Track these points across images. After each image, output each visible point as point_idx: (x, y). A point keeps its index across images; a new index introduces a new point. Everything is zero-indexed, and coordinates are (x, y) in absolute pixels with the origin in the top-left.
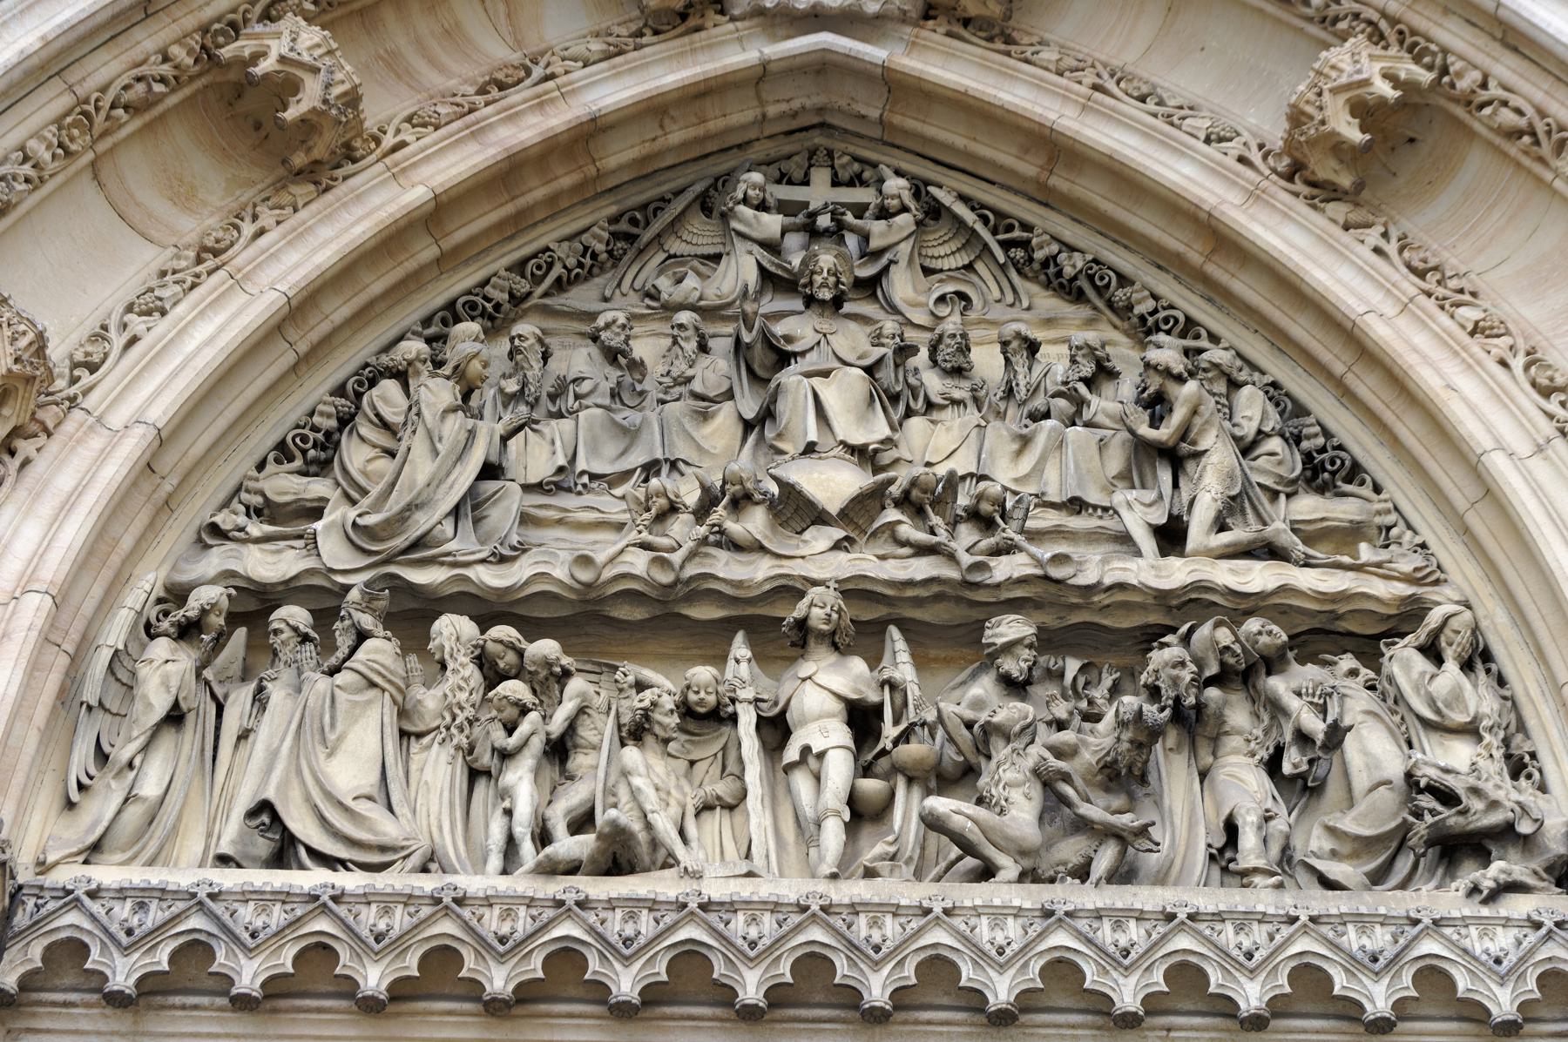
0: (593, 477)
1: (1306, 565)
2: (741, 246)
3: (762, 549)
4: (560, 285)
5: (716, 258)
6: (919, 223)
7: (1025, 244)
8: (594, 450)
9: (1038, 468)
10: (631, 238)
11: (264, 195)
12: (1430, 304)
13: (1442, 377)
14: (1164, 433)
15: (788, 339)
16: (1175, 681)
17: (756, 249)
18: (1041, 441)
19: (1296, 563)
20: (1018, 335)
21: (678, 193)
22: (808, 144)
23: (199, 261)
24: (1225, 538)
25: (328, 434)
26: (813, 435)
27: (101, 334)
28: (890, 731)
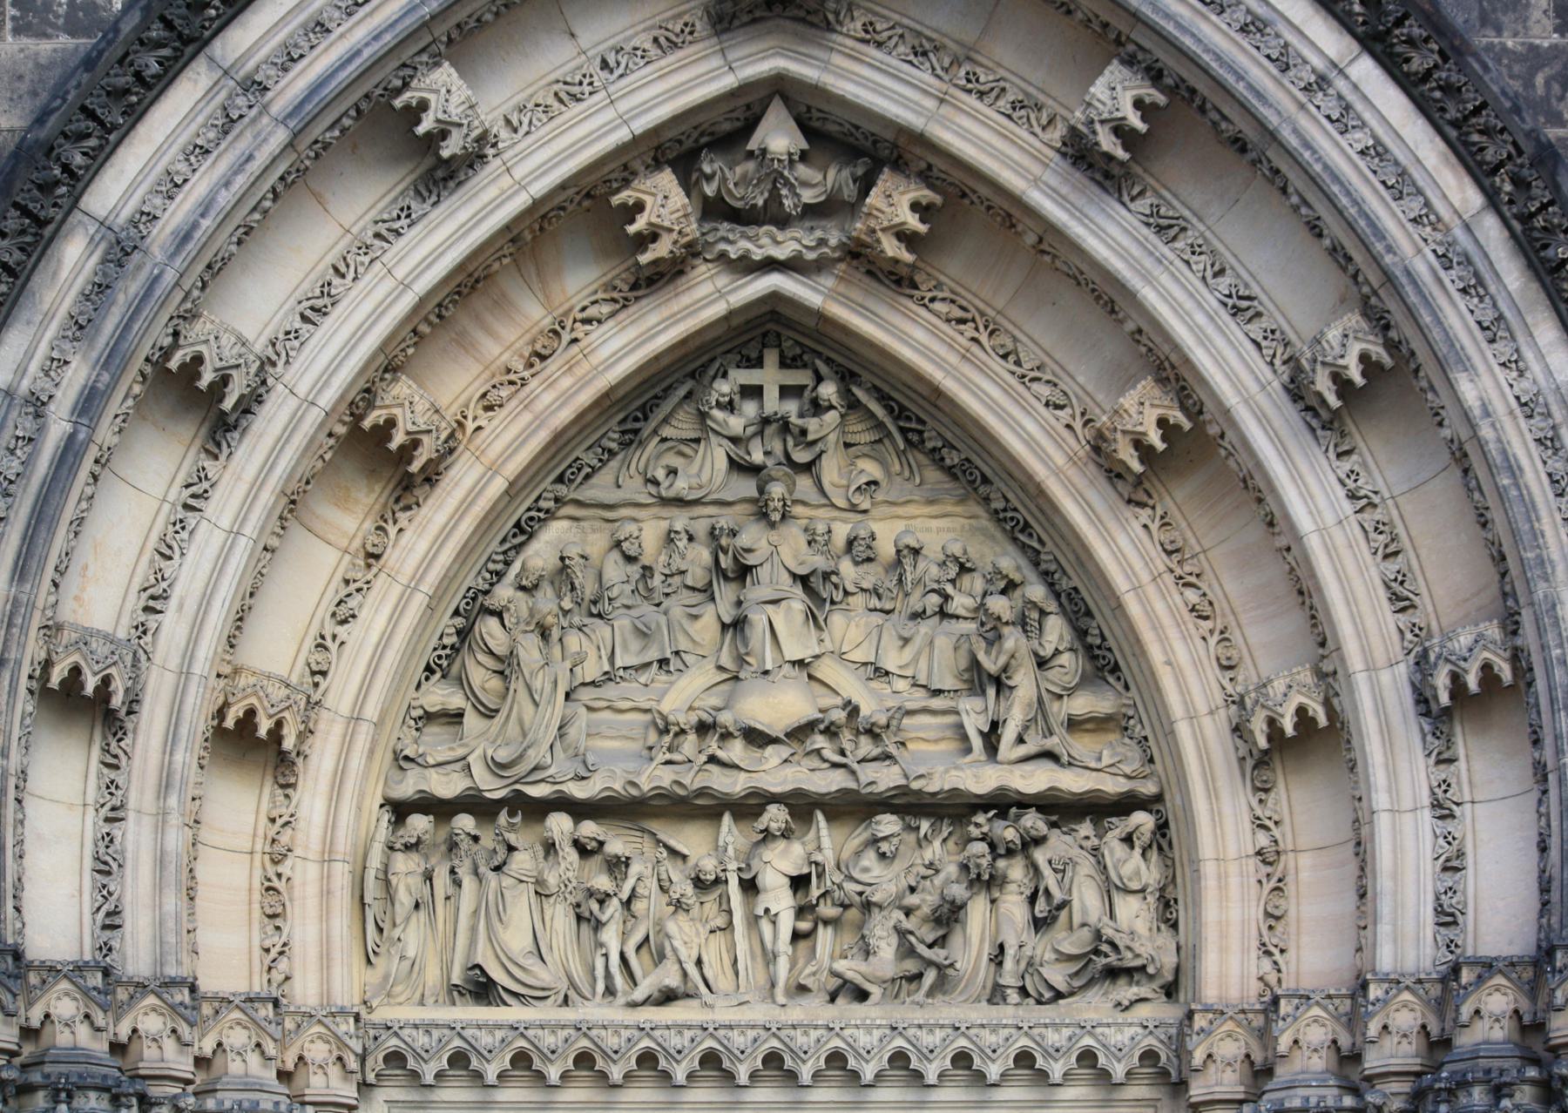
0: (625, 668)
1: (1070, 764)
2: (713, 438)
3: (737, 767)
4: (588, 477)
5: (697, 441)
6: (842, 416)
7: (920, 433)
8: (625, 647)
9: (916, 660)
10: (636, 432)
11: (396, 495)
12: (1169, 579)
13: (1166, 653)
14: (991, 665)
15: (749, 551)
16: (978, 866)
17: (725, 442)
18: (917, 642)
19: (1062, 766)
20: (907, 547)
21: (668, 390)
22: (763, 330)
23: (369, 566)
24: (1022, 751)
25: (453, 647)
26: (769, 666)
27: (321, 646)
28: (815, 892)
